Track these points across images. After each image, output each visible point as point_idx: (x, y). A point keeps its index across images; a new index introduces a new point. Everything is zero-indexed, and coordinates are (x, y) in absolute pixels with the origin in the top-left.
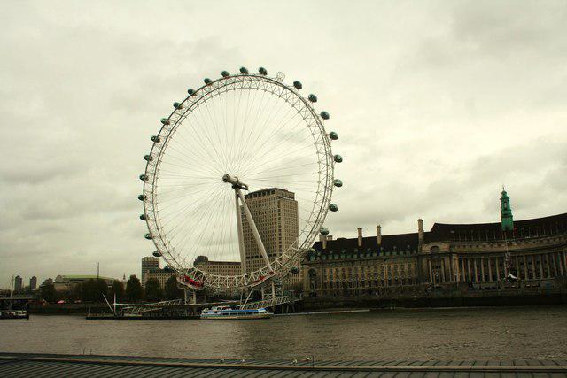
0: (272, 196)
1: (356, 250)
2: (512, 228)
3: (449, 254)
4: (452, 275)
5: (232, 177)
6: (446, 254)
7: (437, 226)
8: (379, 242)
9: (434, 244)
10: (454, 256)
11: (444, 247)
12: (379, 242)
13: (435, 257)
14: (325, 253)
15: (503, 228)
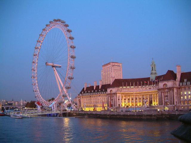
0: (110, 65)
1: (92, 91)
2: (154, 79)
3: (115, 94)
4: (117, 104)
5: (49, 64)
6: (114, 94)
7: (116, 80)
8: (100, 88)
9: (111, 89)
10: (118, 95)
11: (114, 90)
12: (100, 88)
13: (112, 95)
14: (84, 93)
15: (151, 80)
